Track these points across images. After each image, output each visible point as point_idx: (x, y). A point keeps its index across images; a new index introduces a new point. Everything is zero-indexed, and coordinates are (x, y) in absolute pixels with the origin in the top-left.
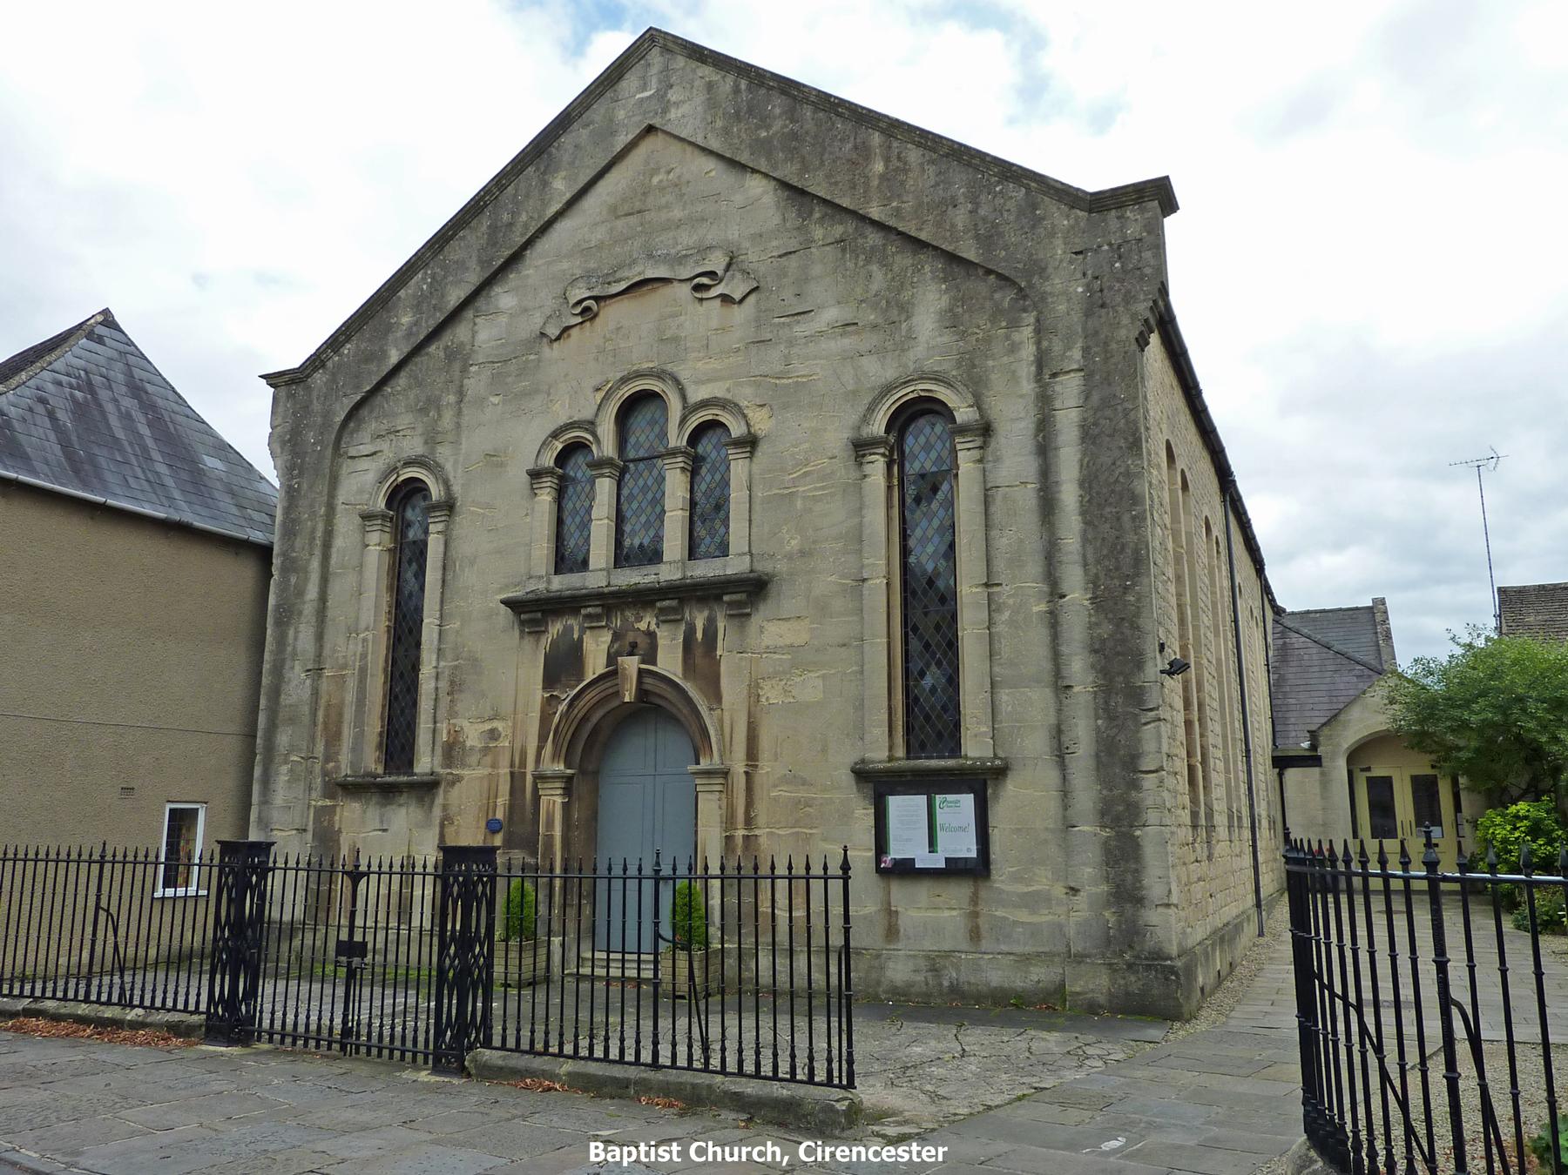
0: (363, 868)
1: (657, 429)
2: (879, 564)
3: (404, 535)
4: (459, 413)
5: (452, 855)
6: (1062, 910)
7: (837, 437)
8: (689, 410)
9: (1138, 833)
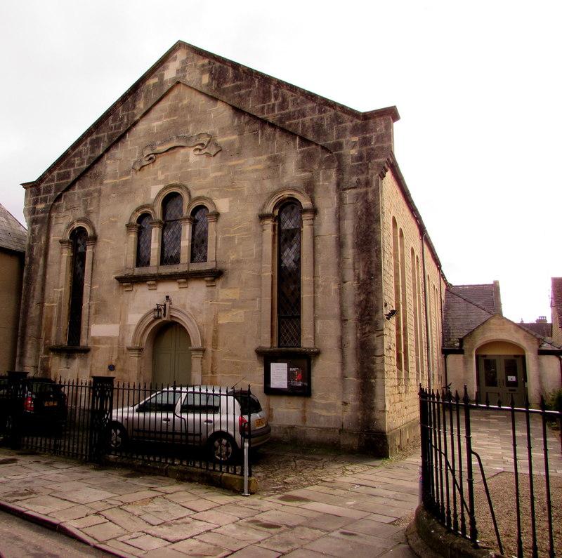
0: (63, 384)
1: (178, 208)
2: (268, 272)
3: (77, 250)
4: (99, 201)
5: (97, 380)
6: (340, 411)
7: (252, 213)
8: (191, 200)
9: (373, 381)
